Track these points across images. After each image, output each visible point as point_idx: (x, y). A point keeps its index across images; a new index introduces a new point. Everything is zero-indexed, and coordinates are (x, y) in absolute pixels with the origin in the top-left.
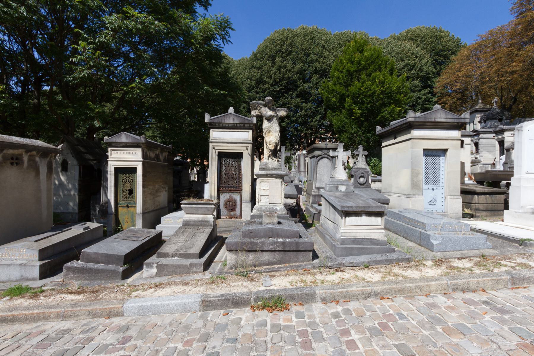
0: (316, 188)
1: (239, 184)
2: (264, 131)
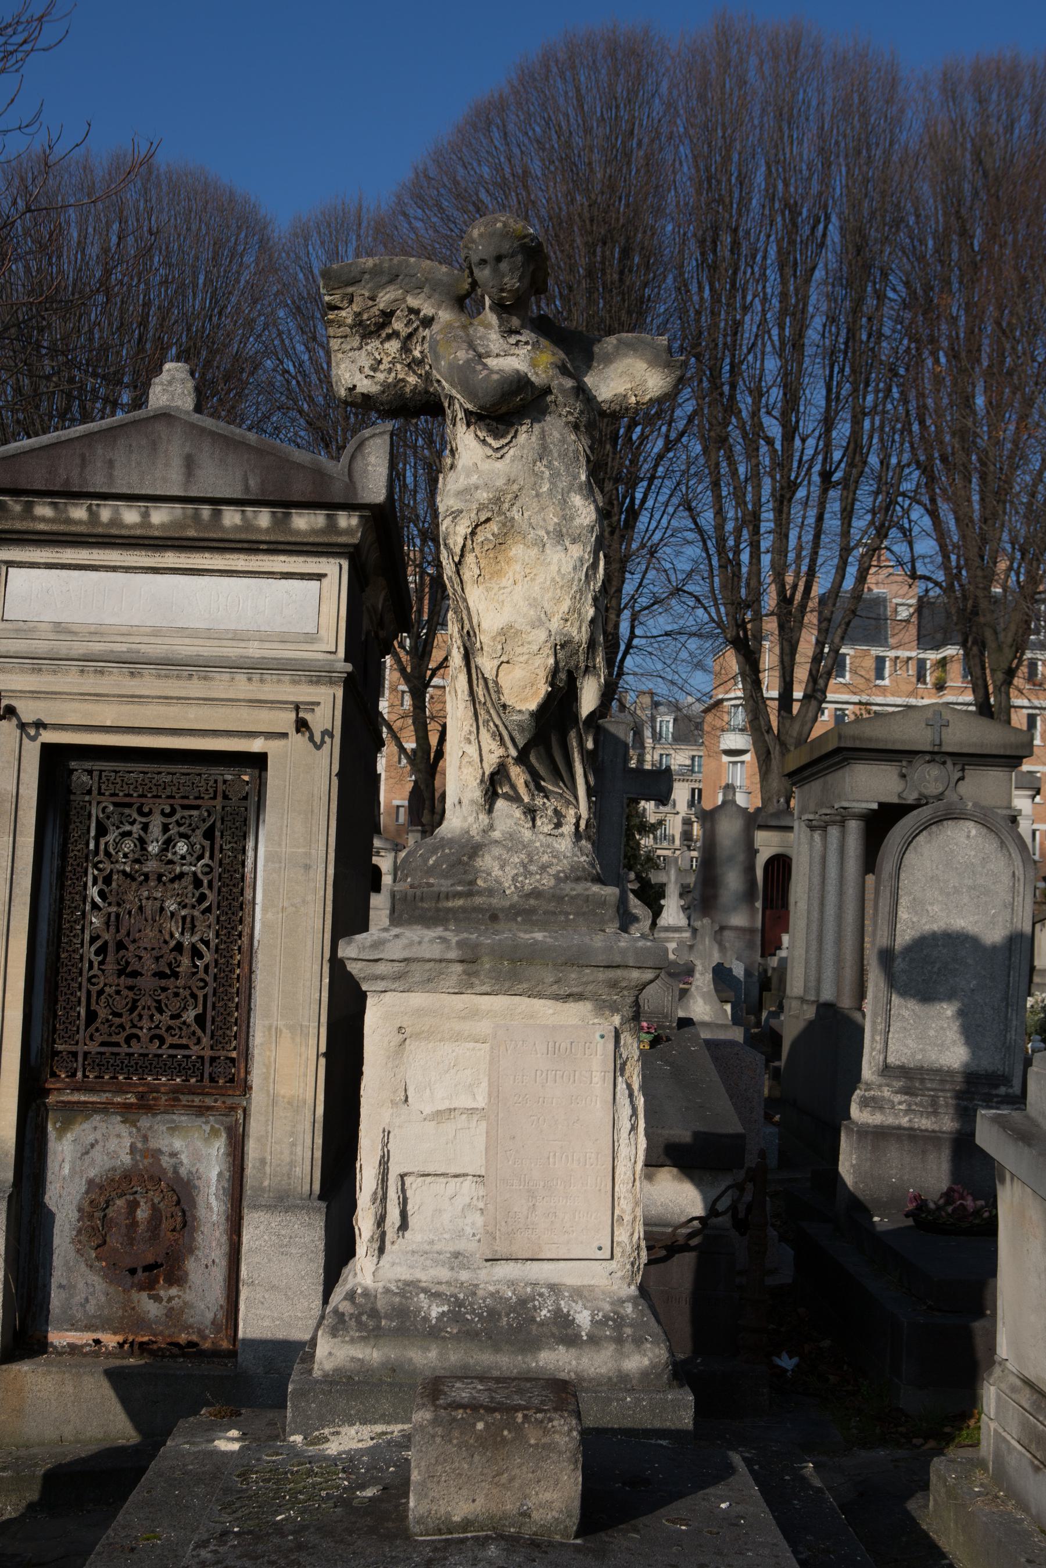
0: (886, 1070)
1: (219, 1040)
2: (455, 533)
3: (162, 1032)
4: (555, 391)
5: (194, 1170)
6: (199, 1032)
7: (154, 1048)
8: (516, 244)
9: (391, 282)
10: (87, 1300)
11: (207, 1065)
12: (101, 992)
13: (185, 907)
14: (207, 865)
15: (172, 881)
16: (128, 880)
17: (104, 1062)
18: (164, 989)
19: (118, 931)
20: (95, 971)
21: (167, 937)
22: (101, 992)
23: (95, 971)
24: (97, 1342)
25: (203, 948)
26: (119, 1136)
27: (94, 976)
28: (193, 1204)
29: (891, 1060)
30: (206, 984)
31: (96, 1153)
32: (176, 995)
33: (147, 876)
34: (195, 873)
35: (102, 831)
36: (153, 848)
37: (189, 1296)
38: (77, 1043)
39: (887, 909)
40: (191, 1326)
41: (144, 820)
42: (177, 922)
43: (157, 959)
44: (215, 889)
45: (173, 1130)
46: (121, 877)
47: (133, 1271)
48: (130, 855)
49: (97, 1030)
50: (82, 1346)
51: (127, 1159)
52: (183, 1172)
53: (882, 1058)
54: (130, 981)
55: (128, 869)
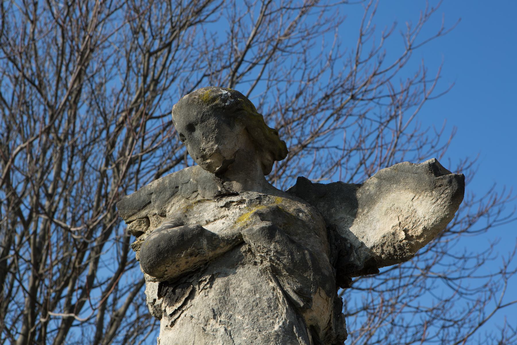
4: (246, 239)
8: (206, 108)
9: (173, 194)
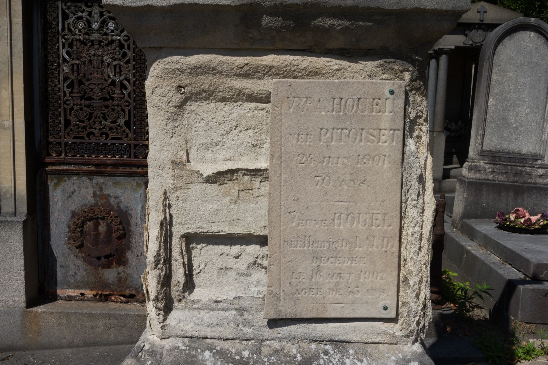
0: (483, 154)
3: (107, 130)
5: (128, 205)
6: (127, 130)
7: (103, 140)
10: (76, 273)
11: (132, 149)
12: (72, 109)
13: (115, 60)
14: (126, 36)
15: (107, 45)
16: (82, 45)
17: (76, 148)
18: (106, 107)
19: (78, 75)
20: (68, 97)
21: (106, 78)
22: (72, 109)
23: (68, 97)
24: (82, 294)
25: (126, 83)
26: (87, 188)
27: (67, 100)
28: (129, 224)
29: (485, 148)
30: (130, 104)
31: (75, 197)
32: (114, 110)
33: (92, 42)
34: (119, 40)
35: (65, 17)
36: (95, 26)
37: (129, 271)
38: (60, 138)
39: (487, 74)
40: (131, 287)
41: (89, 10)
42: (111, 69)
43: (102, 89)
44: (132, 49)
45: (116, 184)
46: (78, 43)
47: (99, 258)
48: (82, 31)
49: (71, 130)
50: (75, 297)
51: (91, 199)
52: (122, 206)
53: (480, 147)
54: (87, 102)
55: (82, 39)
